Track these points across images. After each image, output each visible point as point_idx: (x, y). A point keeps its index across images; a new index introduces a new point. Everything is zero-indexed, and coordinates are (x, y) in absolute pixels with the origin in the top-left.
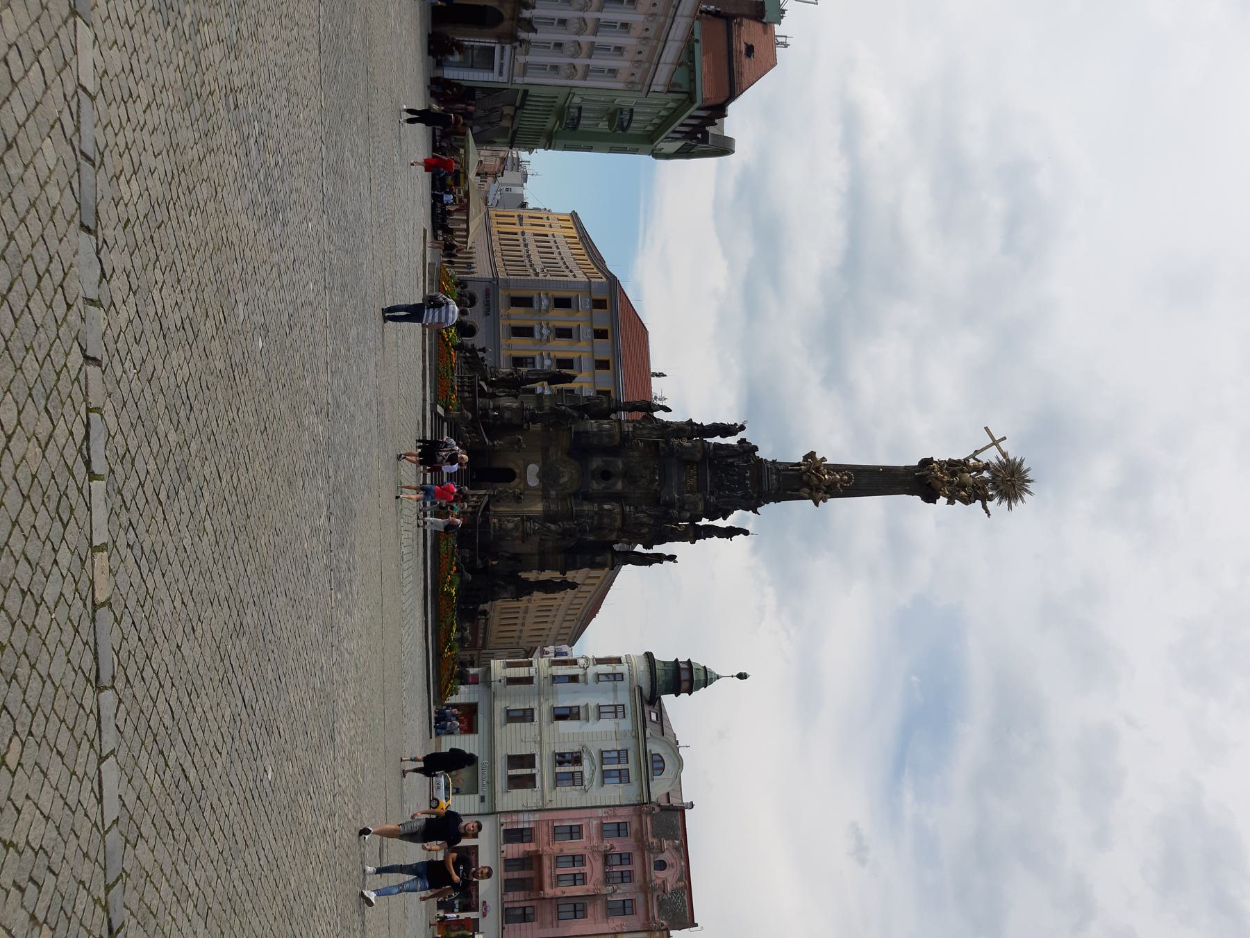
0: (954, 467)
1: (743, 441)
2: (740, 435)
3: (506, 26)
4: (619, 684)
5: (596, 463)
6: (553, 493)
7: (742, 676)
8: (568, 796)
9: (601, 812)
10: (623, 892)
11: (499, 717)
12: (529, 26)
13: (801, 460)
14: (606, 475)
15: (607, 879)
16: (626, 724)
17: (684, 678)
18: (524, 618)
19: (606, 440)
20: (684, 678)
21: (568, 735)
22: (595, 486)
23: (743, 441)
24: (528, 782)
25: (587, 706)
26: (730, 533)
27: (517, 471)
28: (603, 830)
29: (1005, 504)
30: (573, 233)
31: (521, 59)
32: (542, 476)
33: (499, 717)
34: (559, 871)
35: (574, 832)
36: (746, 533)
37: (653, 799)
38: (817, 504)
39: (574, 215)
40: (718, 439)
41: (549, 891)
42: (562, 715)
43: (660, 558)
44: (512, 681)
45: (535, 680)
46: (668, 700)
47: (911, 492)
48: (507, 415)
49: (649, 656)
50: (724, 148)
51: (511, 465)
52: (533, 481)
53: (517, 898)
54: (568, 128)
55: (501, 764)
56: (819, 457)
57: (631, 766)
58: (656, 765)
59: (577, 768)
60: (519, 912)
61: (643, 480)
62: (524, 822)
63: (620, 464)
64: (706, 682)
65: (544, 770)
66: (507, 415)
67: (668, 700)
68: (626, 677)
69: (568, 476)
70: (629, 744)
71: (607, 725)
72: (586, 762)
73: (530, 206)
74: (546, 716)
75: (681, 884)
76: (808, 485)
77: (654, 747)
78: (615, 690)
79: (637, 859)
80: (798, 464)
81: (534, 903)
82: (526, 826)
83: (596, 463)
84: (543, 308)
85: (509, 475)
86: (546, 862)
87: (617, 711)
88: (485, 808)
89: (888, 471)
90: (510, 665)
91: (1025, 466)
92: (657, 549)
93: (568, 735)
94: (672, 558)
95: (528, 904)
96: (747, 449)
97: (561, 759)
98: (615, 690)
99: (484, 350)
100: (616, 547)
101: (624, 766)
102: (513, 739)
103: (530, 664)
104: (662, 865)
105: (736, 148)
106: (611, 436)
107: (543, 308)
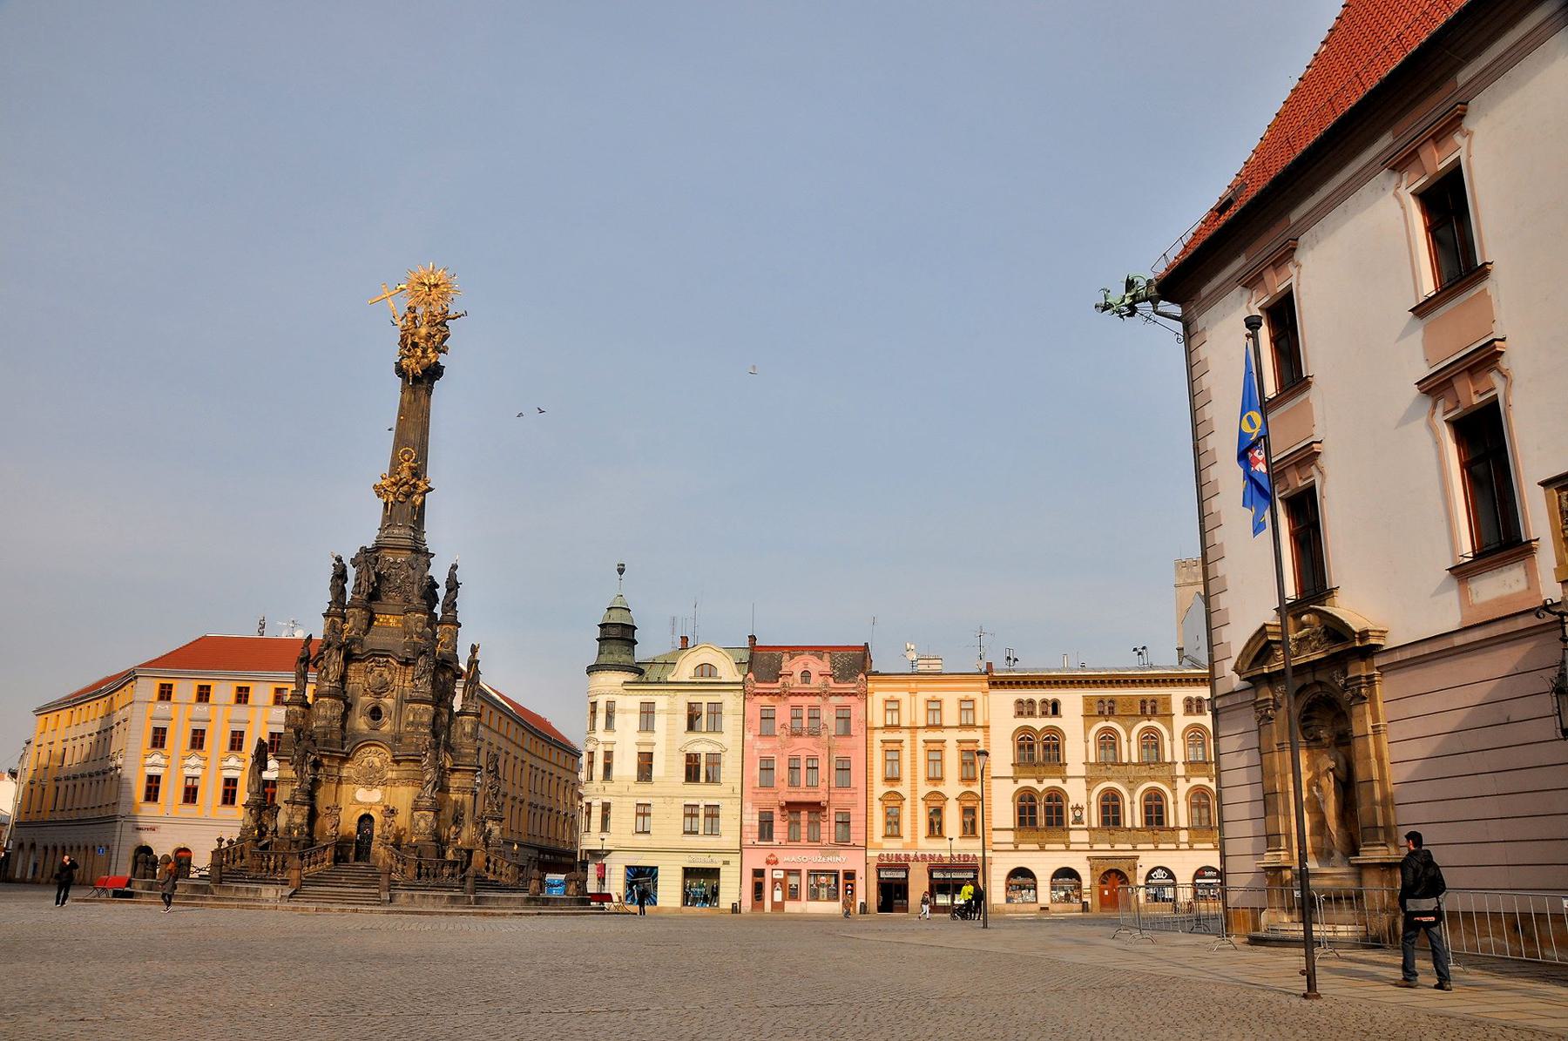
0: (408, 343)
1: (354, 562)
2: (347, 561)
4: (617, 707)
5: (361, 723)
6: (390, 775)
7: (621, 571)
8: (730, 769)
9: (749, 737)
10: (828, 716)
11: (642, 841)
13: (381, 502)
14: (376, 713)
15: (814, 734)
16: (661, 701)
17: (618, 636)
18: (543, 808)
19: (337, 712)
20: (618, 636)
21: (668, 768)
22: (387, 727)
23: (354, 562)
24: (713, 813)
26: (453, 586)
27: (363, 812)
28: (765, 734)
30: (65, 714)
32: (370, 784)
34: (803, 784)
35: (767, 767)
36: (455, 567)
37: (740, 678)
38: (431, 489)
39: (40, 711)
41: (821, 797)
43: (473, 663)
45: (606, 800)
47: (429, 392)
48: (298, 820)
49: (591, 670)
51: (355, 820)
52: (375, 795)
53: (828, 830)
55: (691, 842)
56: (379, 482)
57: (704, 699)
58: (706, 673)
59: (703, 759)
60: (840, 826)
61: (386, 674)
62: (752, 819)
63: (366, 699)
65: (701, 793)
66: (298, 820)
67: (641, 653)
69: (373, 757)
70: (682, 701)
71: (660, 721)
72: (696, 749)
74: (644, 788)
75: (826, 656)
76: (408, 495)
78: (624, 712)
79: (794, 700)
80: (386, 504)
81: (833, 811)
82: (757, 817)
83: (361, 723)
84: (163, 761)
85: (366, 819)
86: (794, 798)
87: (648, 711)
88: (735, 859)
92: (463, 666)
93: (668, 768)
94: (474, 649)
95: (832, 818)
96: (368, 557)
97: (692, 774)
98: (624, 712)
99: (220, 840)
100: (456, 709)
102: (668, 826)
104: (806, 675)
106: (332, 707)
107: (163, 761)
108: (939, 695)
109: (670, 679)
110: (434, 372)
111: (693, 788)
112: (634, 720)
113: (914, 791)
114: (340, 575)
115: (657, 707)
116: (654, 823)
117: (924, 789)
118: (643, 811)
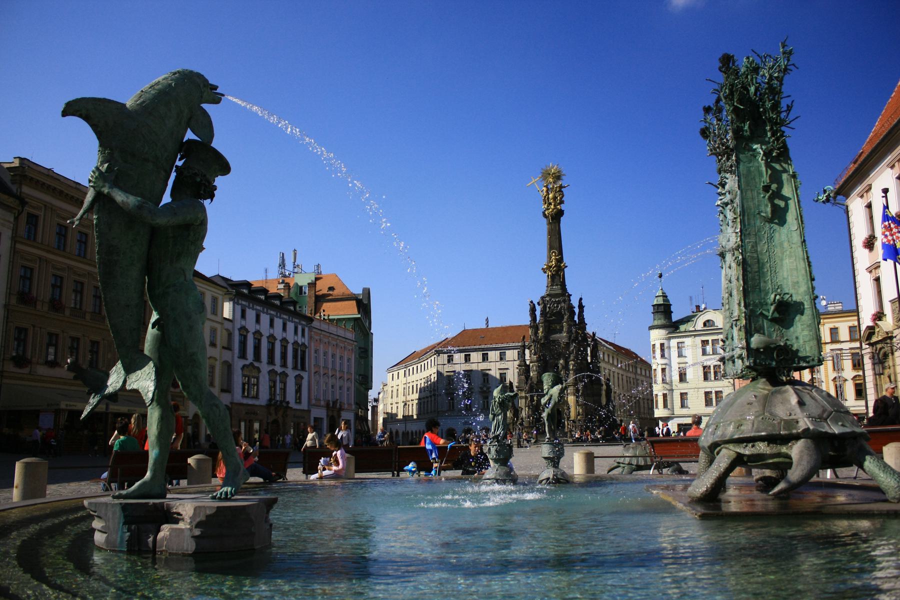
1: (538, 303)
2: (535, 303)
3: (335, 414)
7: (661, 276)
12: (335, 403)
23: (538, 303)
25: (679, 364)
26: (581, 307)
29: (563, 177)
31: (346, 406)
33: (684, 411)
36: (581, 299)
40: (538, 313)
42: (682, 377)
44: (665, 406)
46: (675, 317)
50: (367, 292)
54: (365, 380)
57: (710, 338)
59: (712, 368)
64: (665, 296)
67: (675, 317)
68: (662, 342)
71: (687, 352)
73: (376, 397)
74: (684, 385)
77: (699, 325)
89: (550, 233)
90: (657, 407)
91: (544, 168)
101: (710, 342)
103: (657, 395)
105: (367, 286)
108: (837, 325)
109: (691, 329)
110: (560, 213)
111: (707, 384)
112: (674, 352)
113: (827, 376)
114: (533, 310)
115: (686, 344)
116: (690, 401)
117: (833, 375)
118: (683, 396)
